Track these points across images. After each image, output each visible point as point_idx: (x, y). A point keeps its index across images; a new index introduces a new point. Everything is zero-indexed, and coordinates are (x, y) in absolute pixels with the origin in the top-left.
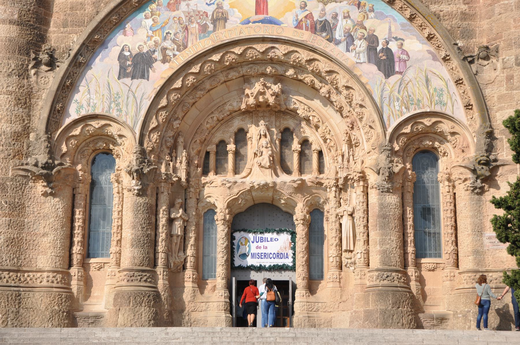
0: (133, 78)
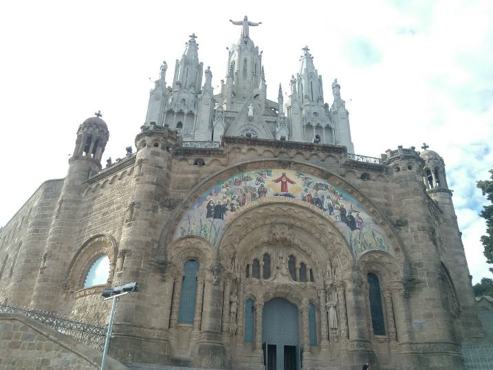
0: (214, 218)
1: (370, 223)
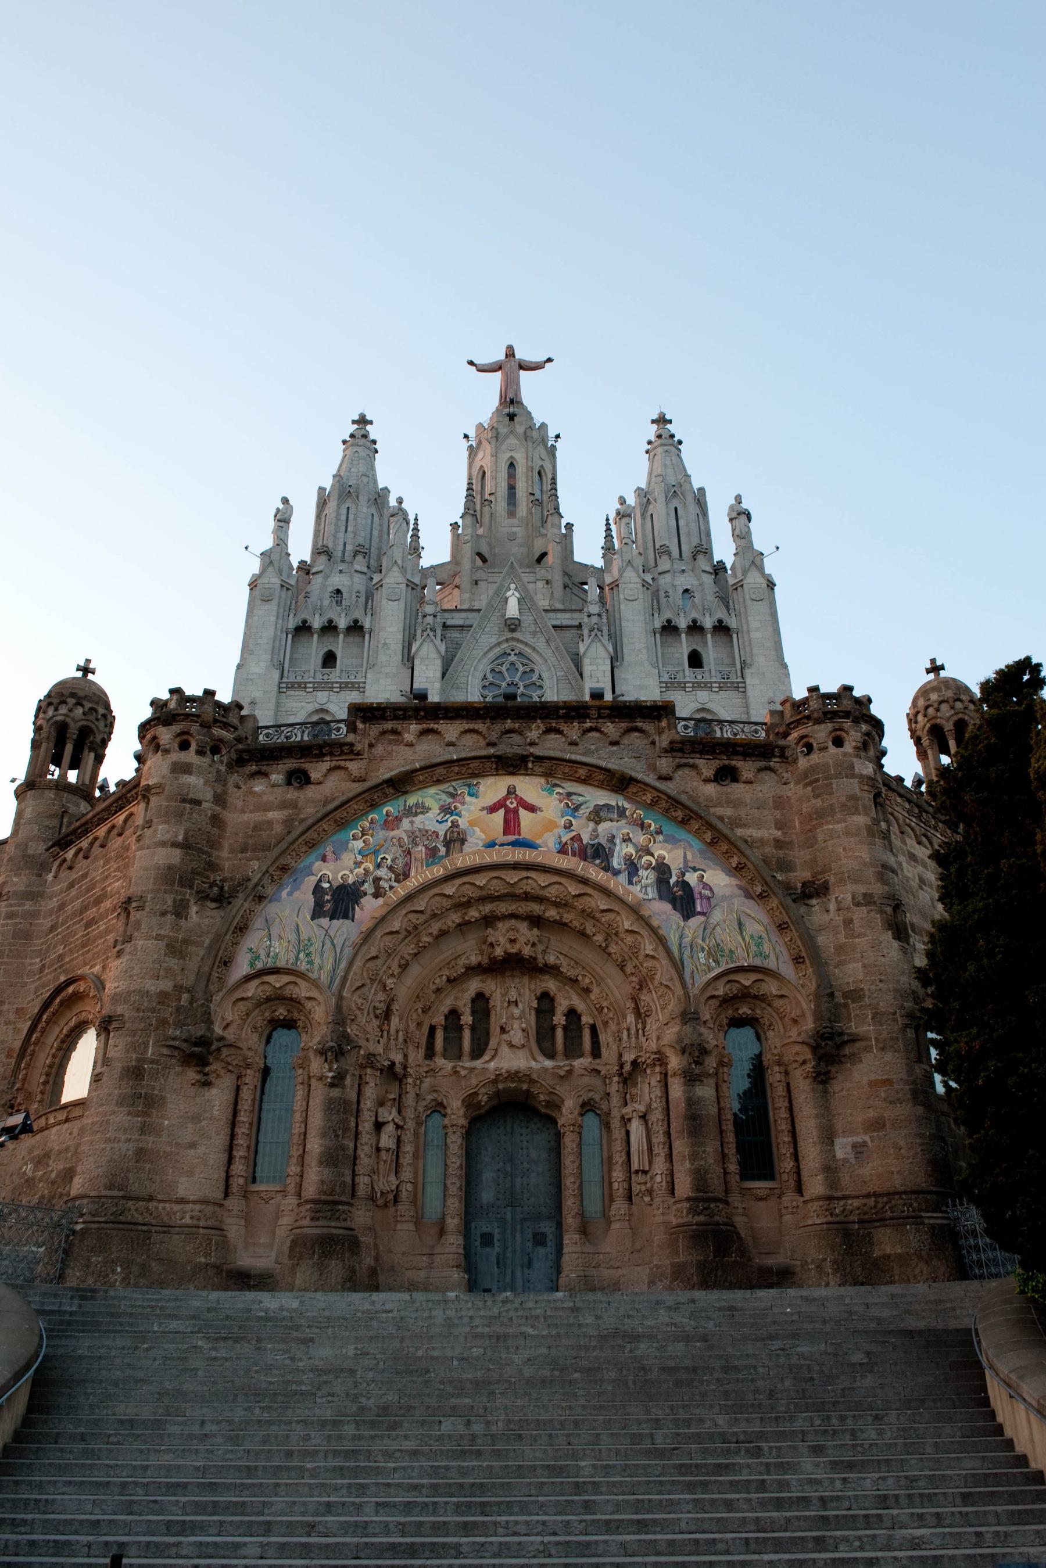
1: (731, 897)
